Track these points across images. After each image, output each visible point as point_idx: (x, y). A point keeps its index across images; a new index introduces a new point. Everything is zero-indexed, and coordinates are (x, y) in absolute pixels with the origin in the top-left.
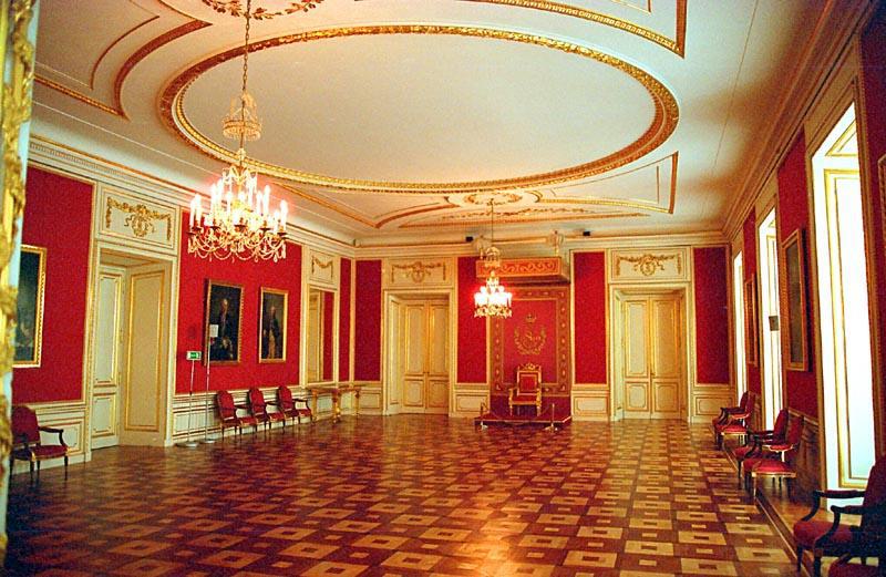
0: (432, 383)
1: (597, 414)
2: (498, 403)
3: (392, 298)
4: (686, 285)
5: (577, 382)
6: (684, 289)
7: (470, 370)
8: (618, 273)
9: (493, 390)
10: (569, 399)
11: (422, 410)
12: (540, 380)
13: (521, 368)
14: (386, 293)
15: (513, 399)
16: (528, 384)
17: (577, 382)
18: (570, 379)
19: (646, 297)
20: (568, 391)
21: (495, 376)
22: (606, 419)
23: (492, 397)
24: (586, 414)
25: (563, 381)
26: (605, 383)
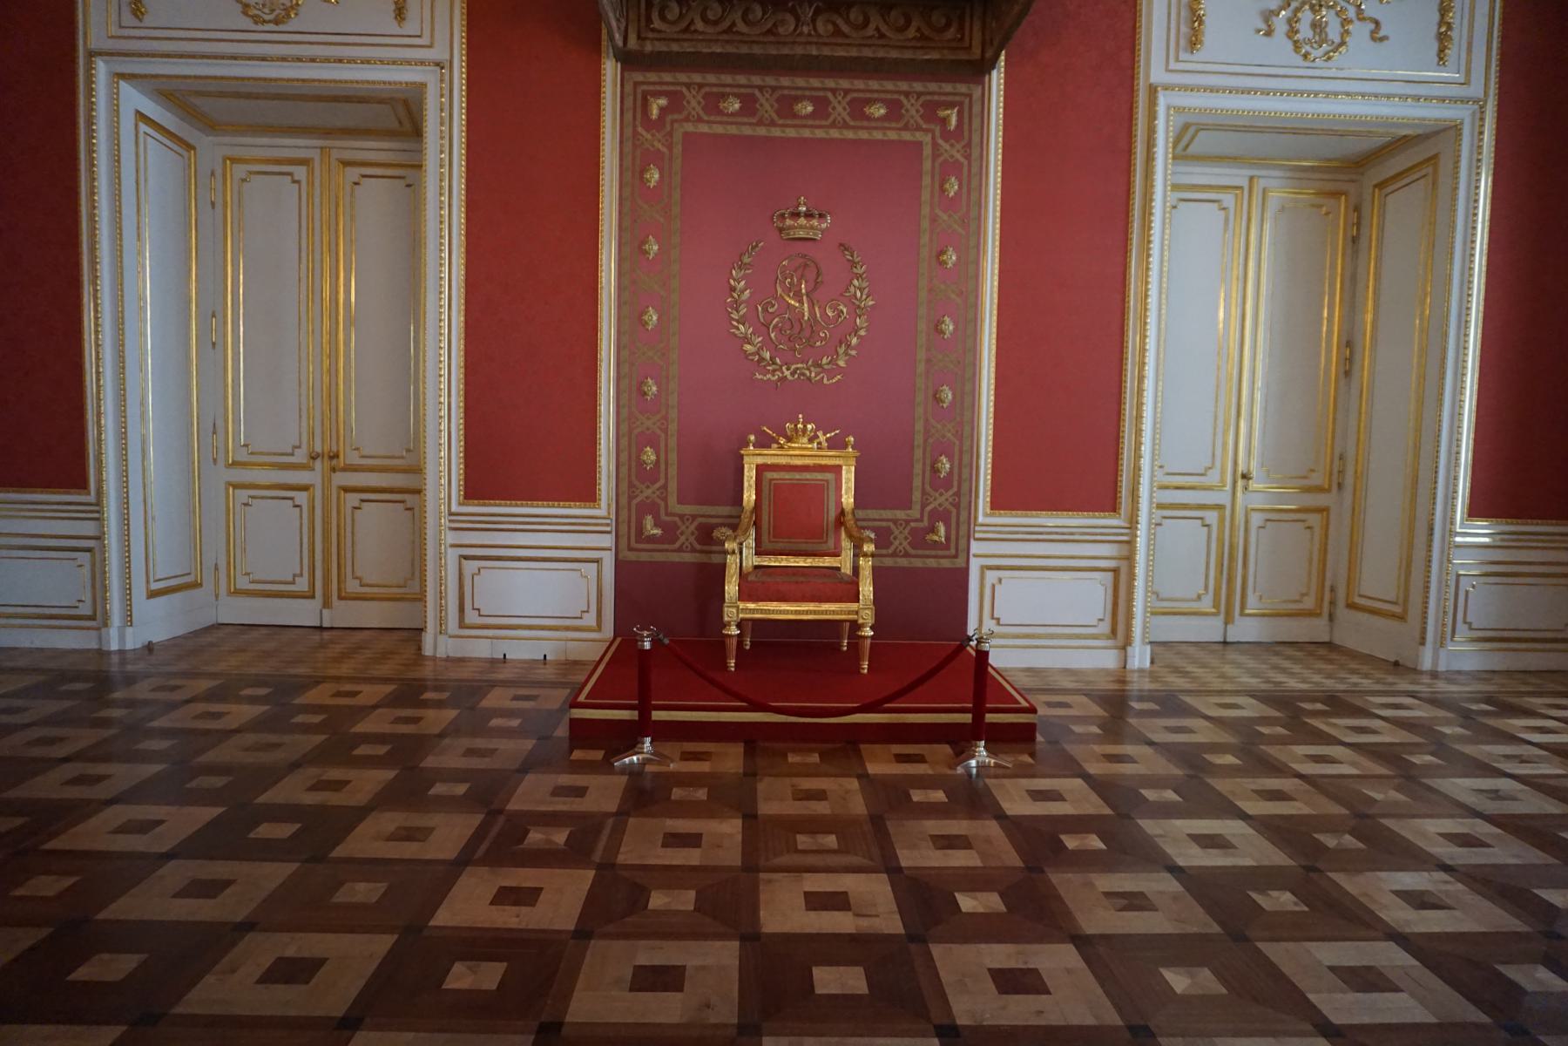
0: (353, 499)
1: (1076, 636)
2: (636, 590)
3: (133, 99)
4: (1463, 113)
5: (997, 504)
6: (1455, 129)
7: (520, 452)
8: (1194, 42)
9: (628, 530)
10: (965, 572)
11: (304, 613)
12: (848, 500)
13: (765, 442)
14: (101, 69)
15: (746, 594)
16: (795, 515)
17: (997, 504)
18: (973, 492)
19: (1238, 176)
20: (958, 545)
21: (634, 474)
22: (1107, 659)
23: (619, 565)
24: (1031, 635)
25: (942, 500)
26: (1113, 508)
